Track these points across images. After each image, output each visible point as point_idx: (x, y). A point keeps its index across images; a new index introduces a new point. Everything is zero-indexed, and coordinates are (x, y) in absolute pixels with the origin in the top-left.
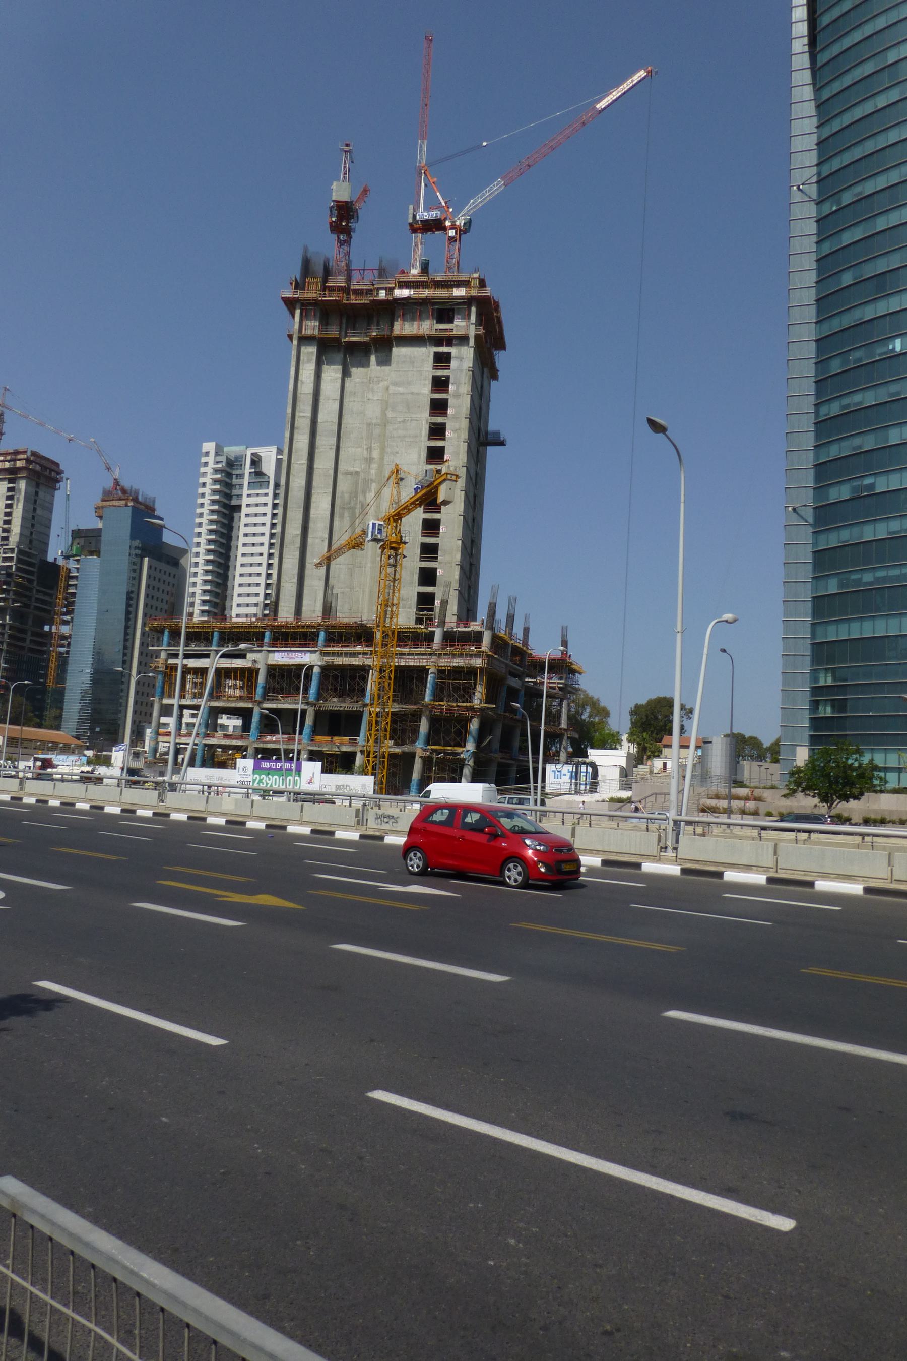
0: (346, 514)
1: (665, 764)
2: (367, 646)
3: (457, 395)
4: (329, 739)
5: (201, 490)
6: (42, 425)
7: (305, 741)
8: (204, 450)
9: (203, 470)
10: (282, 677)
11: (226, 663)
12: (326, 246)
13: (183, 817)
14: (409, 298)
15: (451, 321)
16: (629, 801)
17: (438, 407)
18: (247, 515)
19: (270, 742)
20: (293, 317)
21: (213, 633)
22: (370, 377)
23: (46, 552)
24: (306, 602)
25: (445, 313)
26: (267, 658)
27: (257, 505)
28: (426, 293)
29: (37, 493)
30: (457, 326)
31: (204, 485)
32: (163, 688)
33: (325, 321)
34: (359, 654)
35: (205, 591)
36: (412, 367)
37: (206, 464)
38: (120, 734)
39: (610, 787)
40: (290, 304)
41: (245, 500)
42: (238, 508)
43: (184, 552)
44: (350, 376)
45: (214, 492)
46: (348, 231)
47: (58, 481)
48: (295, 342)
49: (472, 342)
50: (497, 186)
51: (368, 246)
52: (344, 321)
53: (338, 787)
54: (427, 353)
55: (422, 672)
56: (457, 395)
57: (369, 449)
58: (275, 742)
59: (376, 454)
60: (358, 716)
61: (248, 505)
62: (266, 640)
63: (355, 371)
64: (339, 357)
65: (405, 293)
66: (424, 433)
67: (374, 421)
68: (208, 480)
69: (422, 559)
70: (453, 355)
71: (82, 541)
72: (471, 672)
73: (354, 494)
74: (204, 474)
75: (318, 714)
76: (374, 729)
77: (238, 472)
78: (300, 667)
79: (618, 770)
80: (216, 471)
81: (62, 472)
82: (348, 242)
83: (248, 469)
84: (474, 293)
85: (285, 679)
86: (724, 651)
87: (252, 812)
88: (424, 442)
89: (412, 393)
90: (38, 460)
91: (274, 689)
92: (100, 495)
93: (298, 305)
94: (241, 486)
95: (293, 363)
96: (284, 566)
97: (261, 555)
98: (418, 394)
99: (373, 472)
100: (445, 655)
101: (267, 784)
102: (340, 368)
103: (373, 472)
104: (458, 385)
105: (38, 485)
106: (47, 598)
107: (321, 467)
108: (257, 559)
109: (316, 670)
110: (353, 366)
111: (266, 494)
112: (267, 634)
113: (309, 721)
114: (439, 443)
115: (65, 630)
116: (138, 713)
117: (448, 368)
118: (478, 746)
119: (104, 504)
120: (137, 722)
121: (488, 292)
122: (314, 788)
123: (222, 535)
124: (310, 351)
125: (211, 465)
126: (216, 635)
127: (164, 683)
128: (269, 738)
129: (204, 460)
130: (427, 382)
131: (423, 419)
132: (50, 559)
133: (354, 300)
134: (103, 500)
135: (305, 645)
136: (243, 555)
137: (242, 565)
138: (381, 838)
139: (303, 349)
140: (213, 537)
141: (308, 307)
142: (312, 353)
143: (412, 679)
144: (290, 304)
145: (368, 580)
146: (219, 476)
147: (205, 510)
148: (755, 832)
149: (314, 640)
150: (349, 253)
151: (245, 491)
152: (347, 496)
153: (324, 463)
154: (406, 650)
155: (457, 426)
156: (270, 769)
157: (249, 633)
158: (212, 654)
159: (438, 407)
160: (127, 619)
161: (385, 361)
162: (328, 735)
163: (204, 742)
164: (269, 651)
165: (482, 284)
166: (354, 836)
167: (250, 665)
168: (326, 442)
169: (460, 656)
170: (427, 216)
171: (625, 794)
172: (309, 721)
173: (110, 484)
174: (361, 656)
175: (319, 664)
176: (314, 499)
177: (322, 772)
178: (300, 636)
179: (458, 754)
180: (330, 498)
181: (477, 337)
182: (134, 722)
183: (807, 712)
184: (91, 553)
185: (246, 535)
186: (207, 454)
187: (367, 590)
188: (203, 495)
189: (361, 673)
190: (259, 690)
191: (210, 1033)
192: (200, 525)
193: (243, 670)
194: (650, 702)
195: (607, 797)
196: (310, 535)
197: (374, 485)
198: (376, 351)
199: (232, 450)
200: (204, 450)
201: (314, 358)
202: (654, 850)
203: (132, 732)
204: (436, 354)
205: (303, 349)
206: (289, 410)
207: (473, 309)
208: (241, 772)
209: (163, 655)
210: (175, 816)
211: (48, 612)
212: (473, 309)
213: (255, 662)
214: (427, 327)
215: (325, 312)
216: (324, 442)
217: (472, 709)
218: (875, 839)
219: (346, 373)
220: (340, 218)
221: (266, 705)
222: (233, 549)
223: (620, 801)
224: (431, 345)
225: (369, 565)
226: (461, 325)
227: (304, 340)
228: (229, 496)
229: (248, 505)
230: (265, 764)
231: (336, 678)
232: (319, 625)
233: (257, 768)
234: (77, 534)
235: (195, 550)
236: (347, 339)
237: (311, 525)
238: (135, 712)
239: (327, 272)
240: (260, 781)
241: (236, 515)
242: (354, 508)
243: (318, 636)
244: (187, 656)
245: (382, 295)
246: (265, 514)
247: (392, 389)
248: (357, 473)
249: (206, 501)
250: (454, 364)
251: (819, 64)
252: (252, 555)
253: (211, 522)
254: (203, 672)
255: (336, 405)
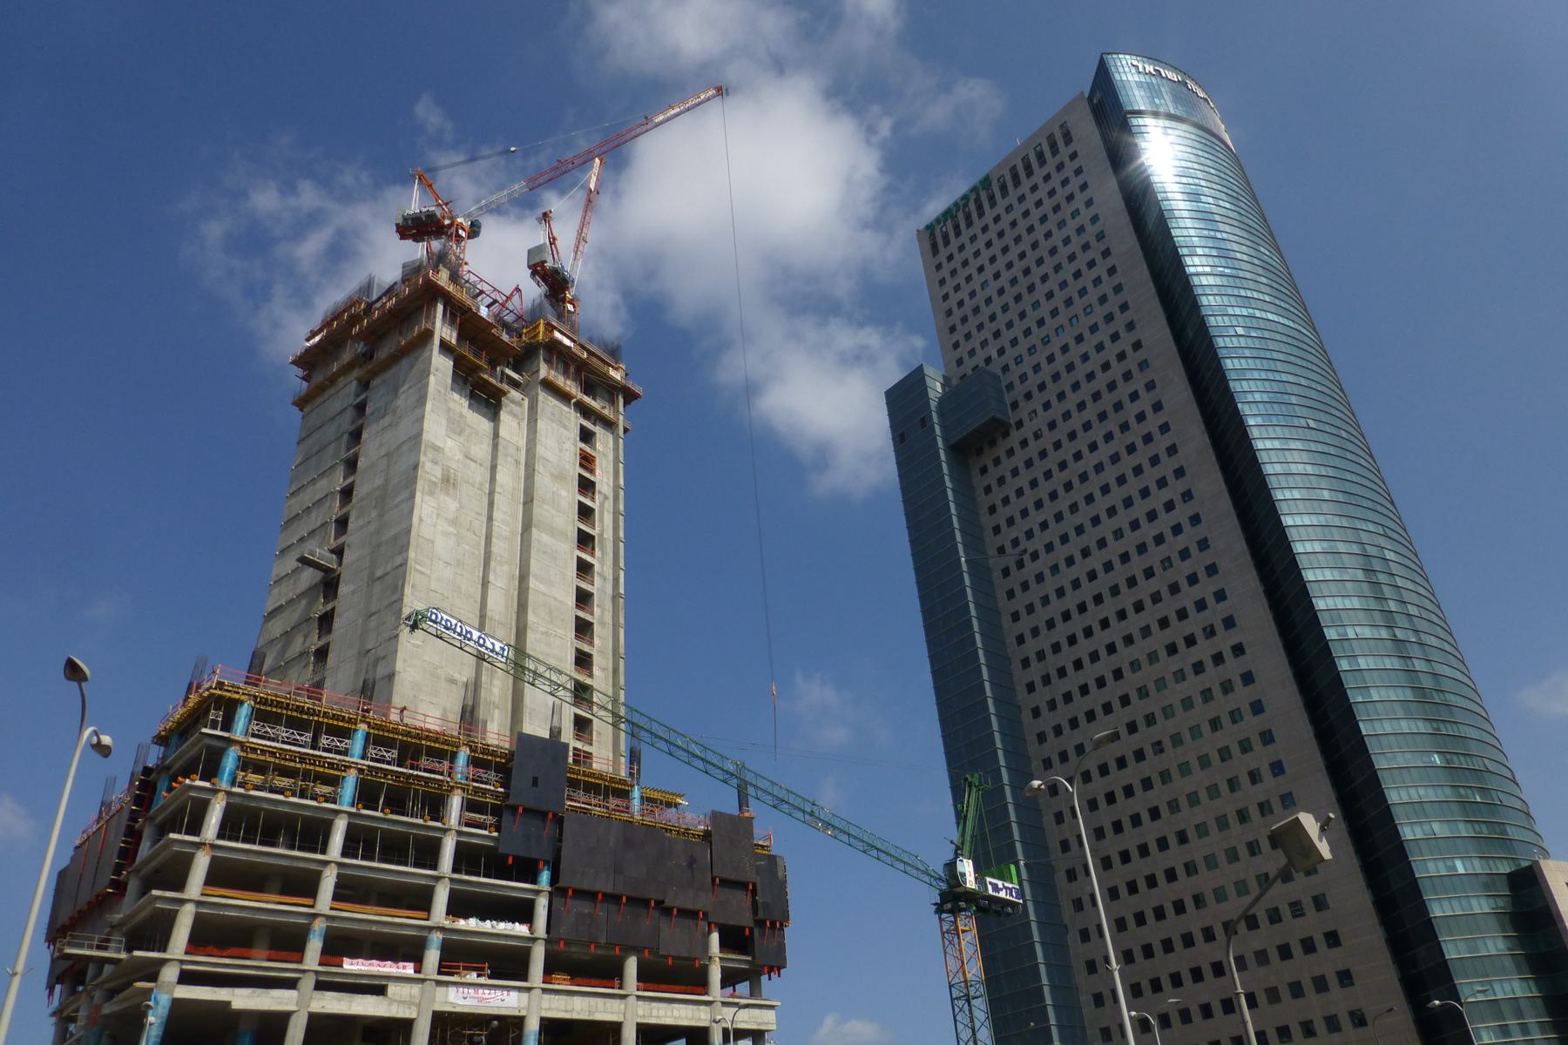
3: (602, 623)
26: (434, 1000)
56: (602, 623)
70: (597, 568)
209: (170, 974)
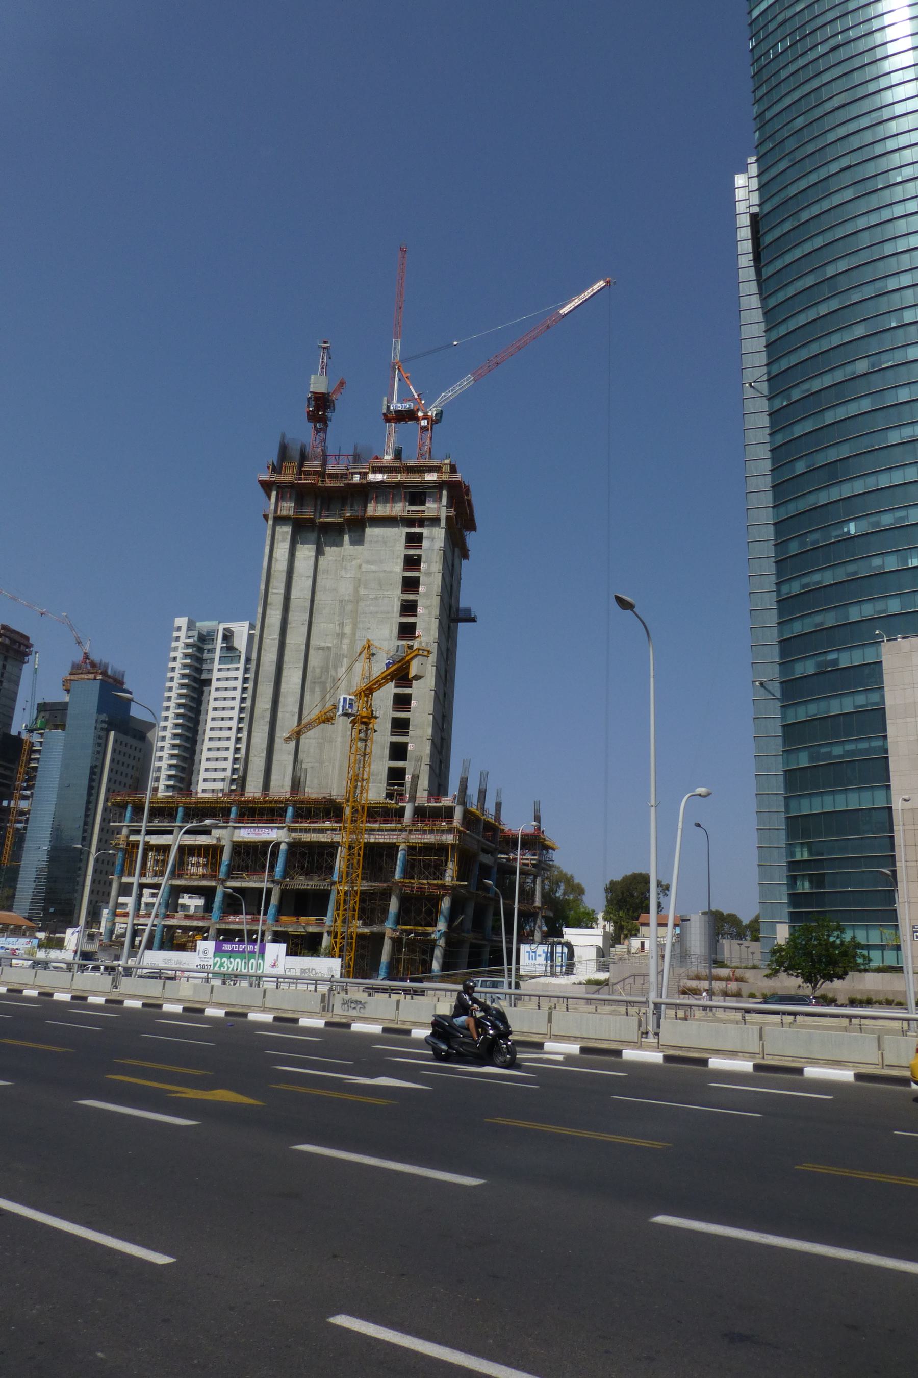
0: (317, 689)
1: (643, 944)
2: (336, 822)
3: (429, 574)
4: (294, 919)
5: (171, 665)
6: (14, 599)
7: (269, 922)
8: (176, 624)
9: (174, 644)
10: (248, 854)
11: (190, 840)
12: (303, 433)
13: (137, 1004)
14: (382, 482)
15: (423, 504)
16: (606, 983)
17: (411, 585)
18: (217, 689)
19: (234, 923)
20: (269, 498)
21: (177, 808)
22: (344, 557)
23: (9, 725)
24: (274, 777)
25: (417, 495)
27: (227, 679)
28: (399, 477)
29: (4, 666)
30: (428, 508)
31: (175, 659)
32: (123, 866)
33: (300, 502)
34: (328, 830)
35: (171, 766)
36: (384, 548)
37: (178, 639)
38: (76, 915)
39: (587, 968)
40: (267, 486)
41: (216, 675)
42: (208, 682)
43: (152, 726)
44: (324, 554)
45: (185, 666)
46: (324, 420)
47: (28, 655)
48: (270, 522)
49: (443, 523)
50: (467, 381)
51: (343, 434)
52: (319, 502)
53: (303, 971)
54: (399, 534)
55: (392, 848)
56: (429, 574)
57: (342, 625)
58: (237, 923)
59: (348, 630)
60: (326, 895)
61: (218, 680)
62: (232, 816)
63: (330, 551)
64: (313, 536)
65: (379, 477)
66: (395, 609)
67: (347, 598)
68: (179, 654)
69: (393, 734)
70: (425, 535)
71: (47, 714)
72: (441, 849)
73: (325, 669)
74: (176, 649)
75: (284, 893)
76: (341, 909)
77: (209, 647)
78: (266, 844)
79: (594, 950)
80: (187, 645)
81: (32, 645)
82: (324, 430)
83: (219, 643)
84: (445, 477)
85: (251, 856)
86: (698, 825)
87: (211, 998)
88: (396, 619)
89: (385, 571)
90: (8, 634)
91: (239, 866)
92: (69, 669)
93: (274, 488)
94: (212, 660)
95: (268, 542)
96: (253, 740)
97: (230, 729)
98: (391, 572)
99: (345, 647)
100: (416, 831)
101: (228, 968)
102: (314, 546)
103: (345, 647)
104: (429, 563)
105: (6, 659)
106: (7, 773)
107: (293, 642)
108: (226, 734)
109: (283, 847)
110: (327, 545)
111: (237, 669)
112: (234, 809)
113: (274, 900)
114: (411, 620)
115: (24, 805)
116: (95, 892)
117: (420, 547)
118: (449, 927)
119: (73, 677)
120: (94, 902)
121: (459, 476)
122: (279, 971)
123: (191, 709)
124: (285, 531)
125: (183, 639)
126: (180, 809)
127: (124, 861)
128: (232, 918)
129: (175, 634)
130: (399, 561)
131: (395, 596)
132: (14, 732)
133: (329, 483)
134: (71, 674)
135: (272, 821)
136: (212, 729)
137: (210, 739)
138: (348, 1026)
139: (278, 528)
140: (181, 711)
141: (283, 490)
142: (287, 532)
143: (381, 856)
144: (267, 486)
145: (338, 755)
146: (190, 651)
147: (175, 684)
148: (738, 1016)
149: (281, 816)
150: (325, 440)
151: (216, 665)
152: (318, 671)
153: (295, 638)
154: (376, 826)
155: (428, 603)
156: (232, 951)
157: (215, 808)
158: (176, 830)
159: (411, 585)
160: (89, 794)
161: (358, 540)
162: (294, 915)
163: (163, 923)
164: (235, 828)
165: (453, 469)
166: (319, 1023)
167: (214, 842)
168: (298, 618)
169: (432, 832)
170: (400, 407)
171: (602, 976)
172: (274, 900)
173: (79, 658)
174: (329, 832)
175: (287, 840)
176: (285, 673)
177: (287, 955)
178: (266, 812)
179: (429, 934)
180: (301, 673)
181: (448, 519)
182: (90, 902)
183: (785, 888)
184: (56, 727)
185: (215, 709)
186: (179, 629)
187: (337, 764)
188: (173, 669)
189: (332, 848)
190: (223, 868)
191: (155, 1250)
192: (169, 699)
193: (207, 847)
194: (626, 879)
195: (583, 978)
196: (280, 710)
197: (345, 660)
198: (349, 531)
199: (204, 625)
200: (176, 624)
201: (289, 537)
202: (635, 1036)
203: (88, 913)
204: (407, 533)
205: (278, 528)
206: (263, 587)
207: (445, 493)
208: (201, 955)
209: (125, 831)
210: (129, 1003)
211: (8, 786)
212: (445, 493)
213: (219, 839)
214: (399, 508)
215: (300, 494)
216: (296, 618)
217: (443, 887)
218: (864, 1021)
219: (319, 552)
220: (317, 408)
221: (229, 884)
222: (201, 724)
223: (597, 983)
224: (403, 526)
225: (339, 739)
226: (431, 508)
227: (280, 520)
228: (199, 671)
229: (218, 680)
230: (227, 947)
231: (303, 855)
232: (287, 800)
233: (218, 950)
234: (43, 708)
235: (162, 724)
236: (321, 520)
237: (281, 699)
238: (92, 892)
239: (303, 457)
240: (222, 965)
241: (206, 689)
242: (324, 683)
243: (286, 812)
244: (149, 833)
245: (357, 479)
246: (235, 689)
247: (365, 567)
248: (329, 648)
249: (176, 675)
250: (425, 544)
251: (764, 278)
252: (221, 729)
253: (180, 696)
254: (166, 849)
255: (309, 582)
